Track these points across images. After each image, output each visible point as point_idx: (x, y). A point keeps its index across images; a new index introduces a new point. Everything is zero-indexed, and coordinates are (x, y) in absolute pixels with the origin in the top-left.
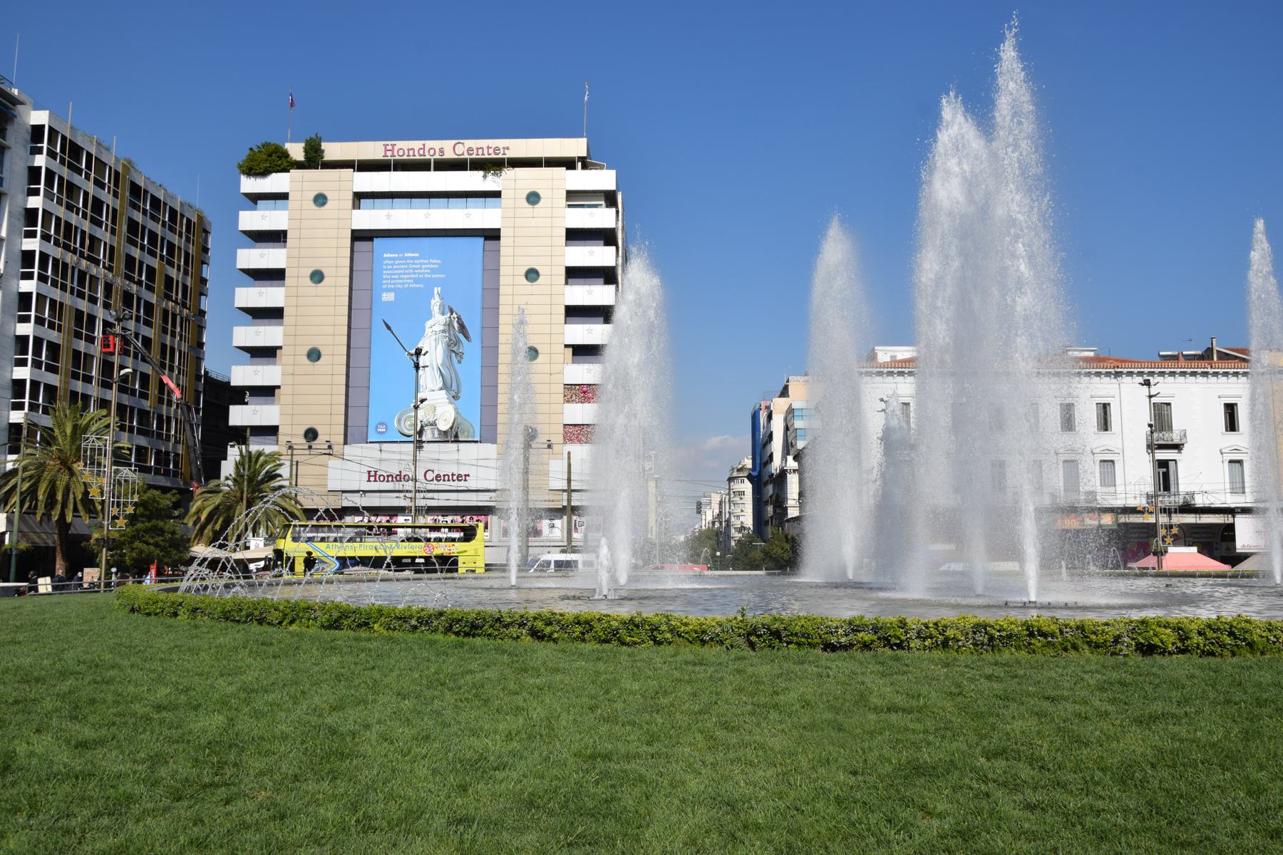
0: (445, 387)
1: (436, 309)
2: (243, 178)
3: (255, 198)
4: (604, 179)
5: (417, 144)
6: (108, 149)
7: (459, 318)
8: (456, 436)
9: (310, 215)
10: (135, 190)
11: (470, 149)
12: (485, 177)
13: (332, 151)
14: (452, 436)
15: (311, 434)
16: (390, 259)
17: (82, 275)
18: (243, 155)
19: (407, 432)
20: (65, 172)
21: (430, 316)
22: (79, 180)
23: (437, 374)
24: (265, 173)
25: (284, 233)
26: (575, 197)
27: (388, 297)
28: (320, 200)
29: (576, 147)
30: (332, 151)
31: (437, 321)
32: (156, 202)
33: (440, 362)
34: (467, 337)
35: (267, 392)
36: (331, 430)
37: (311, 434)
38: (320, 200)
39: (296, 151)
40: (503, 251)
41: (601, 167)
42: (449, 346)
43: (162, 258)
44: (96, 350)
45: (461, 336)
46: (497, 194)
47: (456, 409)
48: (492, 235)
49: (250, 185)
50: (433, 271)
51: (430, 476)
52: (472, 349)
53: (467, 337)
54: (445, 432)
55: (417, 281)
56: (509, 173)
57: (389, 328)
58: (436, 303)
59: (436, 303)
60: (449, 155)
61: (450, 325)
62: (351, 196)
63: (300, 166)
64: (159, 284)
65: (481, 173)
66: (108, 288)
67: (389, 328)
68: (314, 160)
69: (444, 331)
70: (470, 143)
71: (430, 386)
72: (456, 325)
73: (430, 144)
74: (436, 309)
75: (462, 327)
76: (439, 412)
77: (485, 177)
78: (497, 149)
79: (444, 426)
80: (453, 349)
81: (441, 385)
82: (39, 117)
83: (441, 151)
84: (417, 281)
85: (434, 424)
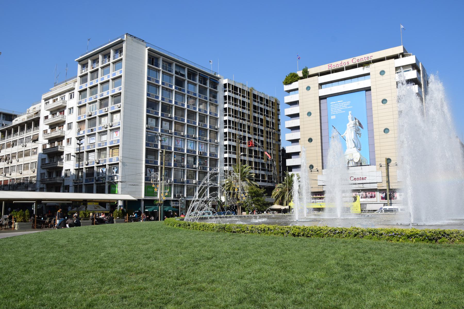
0: (356, 146)
2: (285, 86)
3: (289, 91)
4: (411, 60)
5: (339, 62)
6: (245, 86)
8: (361, 164)
9: (306, 94)
10: (255, 96)
11: (358, 60)
12: (363, 69)
13: (312, 71)
14: (360, 164)
15: (311, 167)
16: (333, 104)
17: (241, 124)
18: (283, 79)
20: (233, 95)
21: (348, 122)
22: (237, 97)
23: (352, 142)
24: (291, 83)
25: (298, 101)
27: (333, 117)
28: (308, 88)
29: (399, 50)
30: (312, 71)
31: (351, 123)
32: (261, 98)
33: (353, 138)
34: (362, 127)
35: (297, 154)
36: (318, 165)
37: (311, 167)
38: (308, 88)
39: (300, 74)
40: (372, 94)
41: (410, 55)
42: (356, 131)
43: (265, 115)
44: (247, 146)
45: (360, 128)
46: (368, 74)
47: (360, 154)
48: (368, 89)
49: (287, 88)
50: (348, 106)
51: (352, 179)
52: (364, 132)
53: (362, 127)
54: (357, 163)
55: (343, 110)
56: (372, 65)
58: (350, 117)
59: (350, 117)
60: (351, 63)
61: (355, 124)
62: (318, 85)
63: (301, 78)
64: (265, 123)
65: (362, 68)
66: (249, 127)
68: (306, 75)
69: (353, 127)
70: (358, 58)
71: (350, 147)
72: (358, 124)
73: (343, 61)
75: (360, 124)
76: (354, 156)
77: (363, 69)
78: (368, 57)
79: (356, 161)
80: (357, 132)
81: (354, 146)
82: (225, 81)
83: (348, 63)
85: (352, 160)
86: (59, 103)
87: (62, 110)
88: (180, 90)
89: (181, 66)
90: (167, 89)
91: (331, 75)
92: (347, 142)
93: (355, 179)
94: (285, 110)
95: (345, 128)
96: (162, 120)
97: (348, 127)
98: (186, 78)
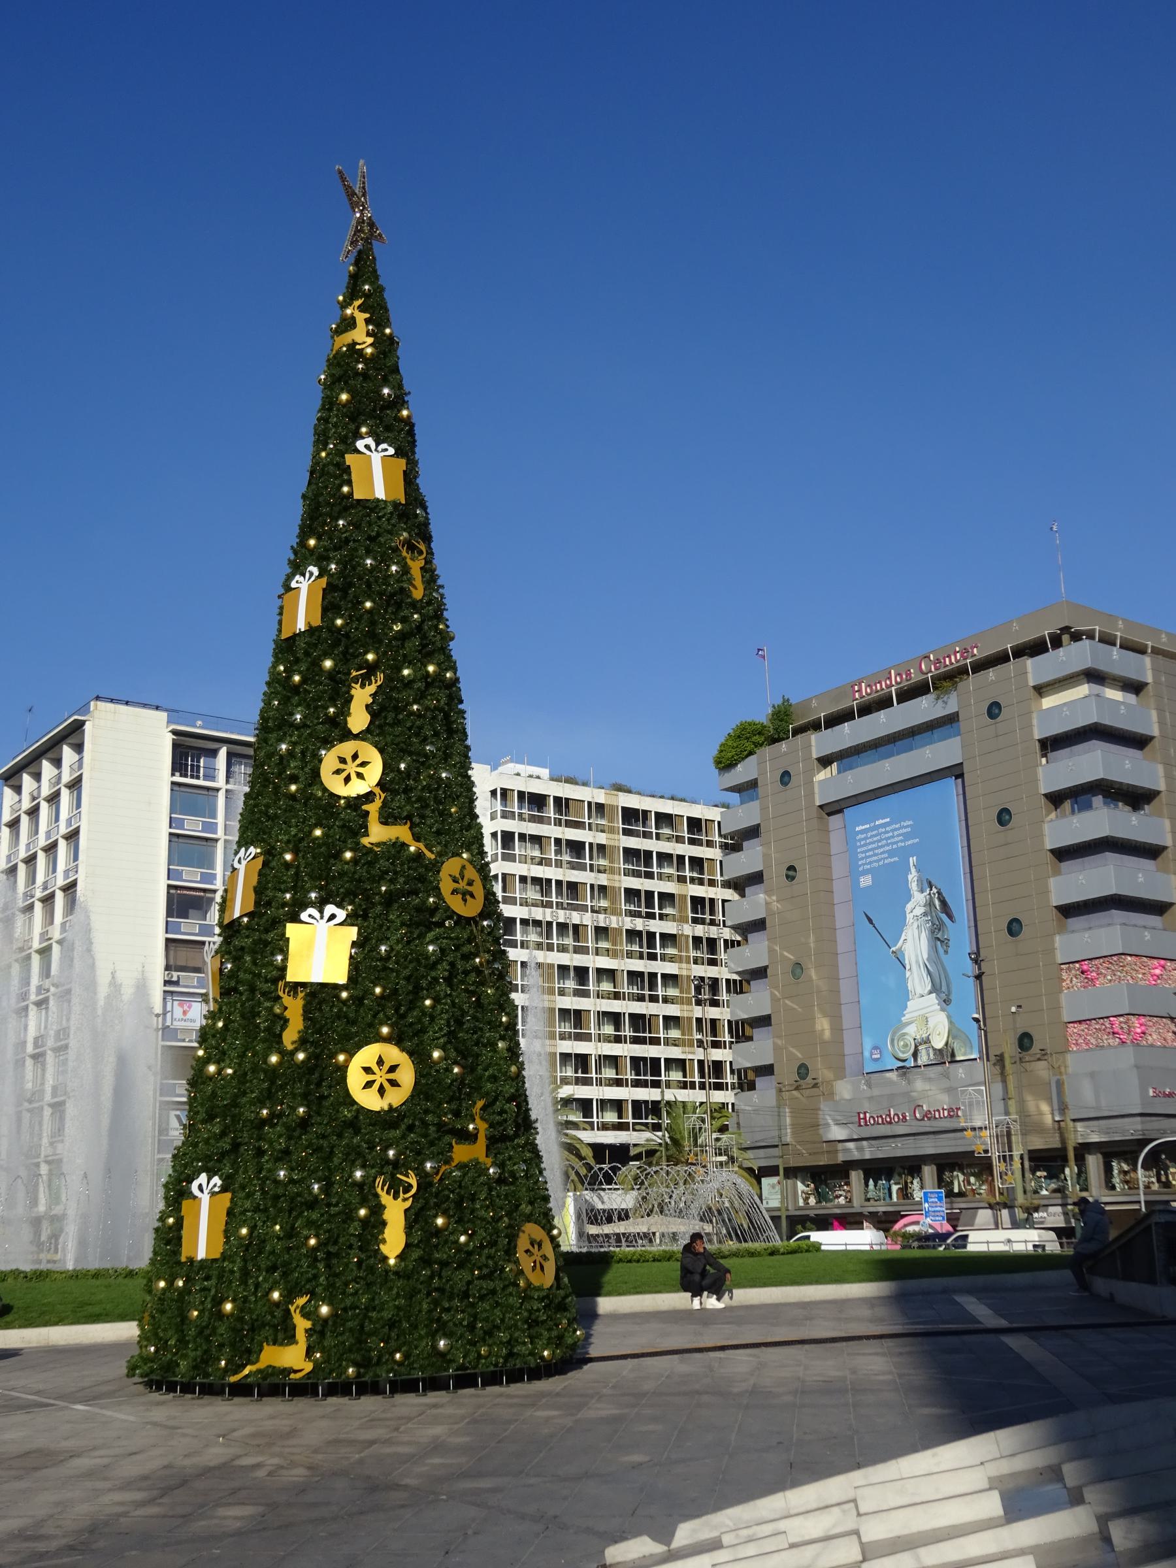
0: (935, 989)
1: (914, 886)
7: (939, 893)
8: (953, 1055)
16: (862, 832)
17: (563, 927)
19: (901, 1056)
21: (909, 897)
23: (925, 974)
27: (866, 881)
31: (917, 903)
33: (925, 956)
34: (950, 917)
42: (932, 932)
45: (944, 917)
47: (949, 1017)
48: (956, 772)
50: (907, 837)
53: (950, 917)
55: (891, 853)
57: (870, 921)
58: (913, 876)
59: (913, 876)
61: (930, 904)
67: (870, 921)
69: (925, 914)
71: (919, 991)
72: (937, 903)
74: (914, 886)
75: (944, 903)
76: (931, 1024)
79: (939, 1044)
80: (938, 938)
81: (929, 987)
84: (891, 853)
85: (927, 1041)
92: (908, 974)
94: (340, 976)
95: (902, 923)
97: (909, 917)
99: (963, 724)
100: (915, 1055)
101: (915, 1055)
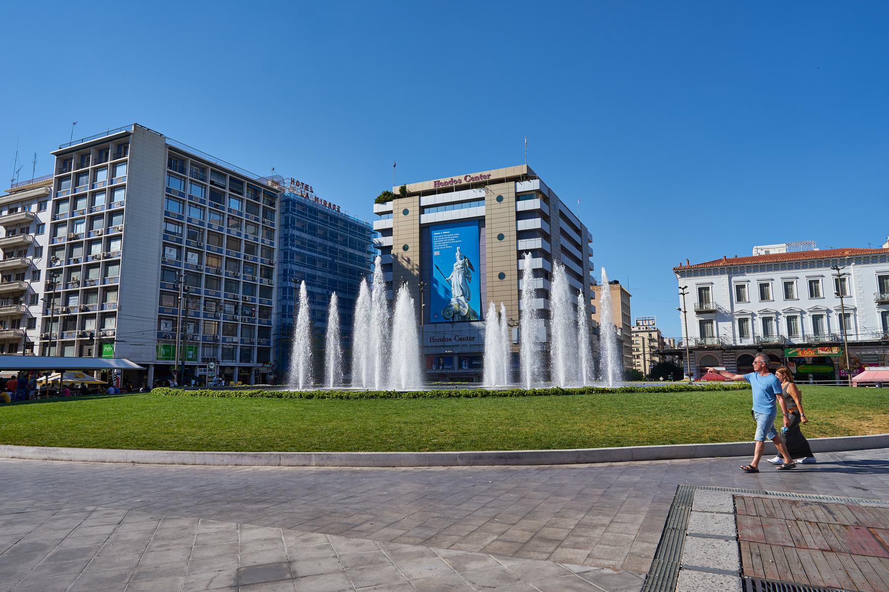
3: (381, 214)
25: (391, 229)
26: (519, 196)
31: (459, 263)
38: (406, 212)
42: (464, 274)
50: (456, 239)
51: (457, 338)
53: (473, 270)
55: (449, 245)
58: (458, 254)
59: (458, 254)
61: (464, 264)
63: (398, 197)
68: (404, 193)
84: (449, 245)
86: (20, 215)
87: (25, 226)
88: (216, 206)
89: (220, 172)
90: (196, 205)
91: (437, 196)
93: (460, 339)
95: (452, 270)
96: (188, 250)
98: (227, 191)
99: (486, 202)
100: (453, 317)
101: (453, 317)
